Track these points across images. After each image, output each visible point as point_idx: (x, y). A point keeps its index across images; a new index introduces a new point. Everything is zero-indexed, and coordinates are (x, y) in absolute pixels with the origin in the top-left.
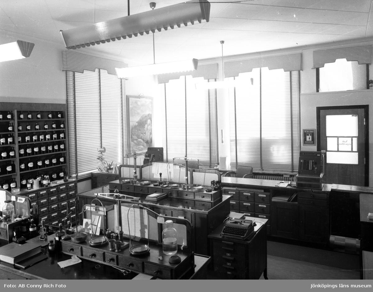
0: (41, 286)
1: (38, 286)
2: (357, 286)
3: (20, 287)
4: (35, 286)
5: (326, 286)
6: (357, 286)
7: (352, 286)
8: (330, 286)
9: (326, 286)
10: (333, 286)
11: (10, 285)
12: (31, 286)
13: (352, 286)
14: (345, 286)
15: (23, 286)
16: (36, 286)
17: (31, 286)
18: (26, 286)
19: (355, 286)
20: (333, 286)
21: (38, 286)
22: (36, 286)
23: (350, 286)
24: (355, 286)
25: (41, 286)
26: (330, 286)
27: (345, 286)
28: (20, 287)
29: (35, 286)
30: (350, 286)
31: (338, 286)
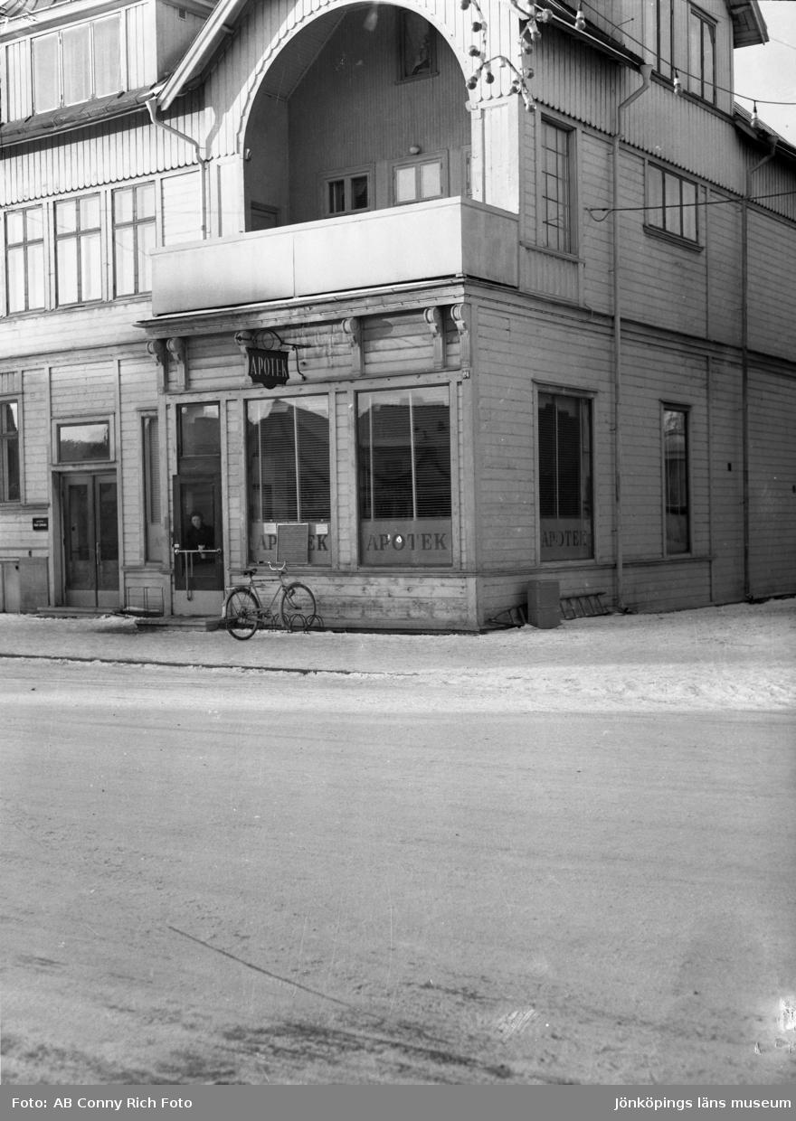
0: (118, 1103)
1: (109, 1104)
2: (748, 1104)
3: (58, 1106)
4: (100, 1104)
5: (658, 1104)
6: (748, 1104)
7: (735, 1103)
8: (671, 1104)
9: (658, 1104)
10: (680, 1104)
11: (177, 1100)
12: (91, 1104)
13: (735, 1103)
14: (714, 1104)
15: (68, 1105)
16: (105, 1104)
17: (91, 1104)
18: (74, 1103)
19: (743, 1104)
20: (680, 1104)
21: (109, 1104)
22: (105, 1104)
23: (728, 1104)
24: (743, 1104)
25: (118, 1103)
26: (671, 1104)
27: (714, 1104)
28: (58, 1106)
29: (100, 1104)
30: (728, 1104)
31: (695, 1103)
